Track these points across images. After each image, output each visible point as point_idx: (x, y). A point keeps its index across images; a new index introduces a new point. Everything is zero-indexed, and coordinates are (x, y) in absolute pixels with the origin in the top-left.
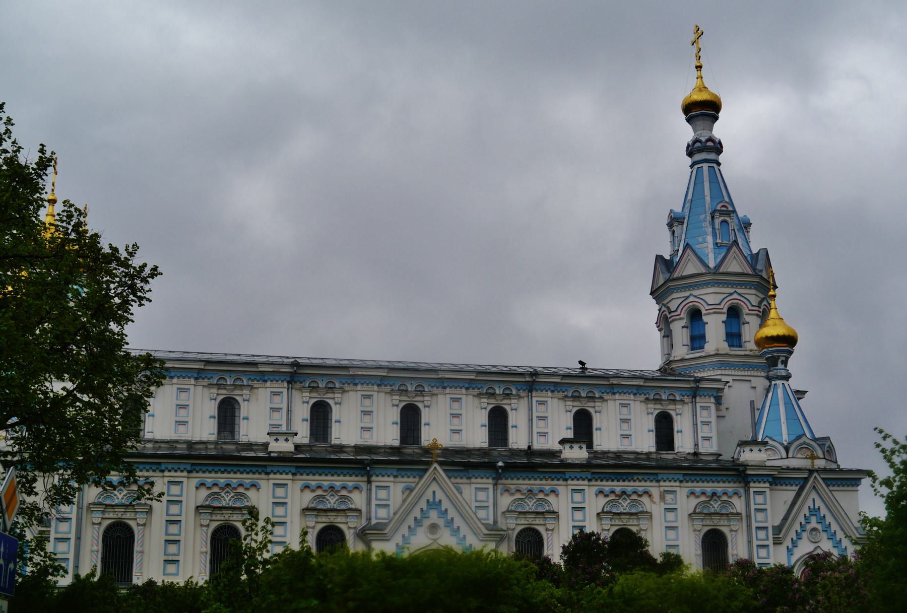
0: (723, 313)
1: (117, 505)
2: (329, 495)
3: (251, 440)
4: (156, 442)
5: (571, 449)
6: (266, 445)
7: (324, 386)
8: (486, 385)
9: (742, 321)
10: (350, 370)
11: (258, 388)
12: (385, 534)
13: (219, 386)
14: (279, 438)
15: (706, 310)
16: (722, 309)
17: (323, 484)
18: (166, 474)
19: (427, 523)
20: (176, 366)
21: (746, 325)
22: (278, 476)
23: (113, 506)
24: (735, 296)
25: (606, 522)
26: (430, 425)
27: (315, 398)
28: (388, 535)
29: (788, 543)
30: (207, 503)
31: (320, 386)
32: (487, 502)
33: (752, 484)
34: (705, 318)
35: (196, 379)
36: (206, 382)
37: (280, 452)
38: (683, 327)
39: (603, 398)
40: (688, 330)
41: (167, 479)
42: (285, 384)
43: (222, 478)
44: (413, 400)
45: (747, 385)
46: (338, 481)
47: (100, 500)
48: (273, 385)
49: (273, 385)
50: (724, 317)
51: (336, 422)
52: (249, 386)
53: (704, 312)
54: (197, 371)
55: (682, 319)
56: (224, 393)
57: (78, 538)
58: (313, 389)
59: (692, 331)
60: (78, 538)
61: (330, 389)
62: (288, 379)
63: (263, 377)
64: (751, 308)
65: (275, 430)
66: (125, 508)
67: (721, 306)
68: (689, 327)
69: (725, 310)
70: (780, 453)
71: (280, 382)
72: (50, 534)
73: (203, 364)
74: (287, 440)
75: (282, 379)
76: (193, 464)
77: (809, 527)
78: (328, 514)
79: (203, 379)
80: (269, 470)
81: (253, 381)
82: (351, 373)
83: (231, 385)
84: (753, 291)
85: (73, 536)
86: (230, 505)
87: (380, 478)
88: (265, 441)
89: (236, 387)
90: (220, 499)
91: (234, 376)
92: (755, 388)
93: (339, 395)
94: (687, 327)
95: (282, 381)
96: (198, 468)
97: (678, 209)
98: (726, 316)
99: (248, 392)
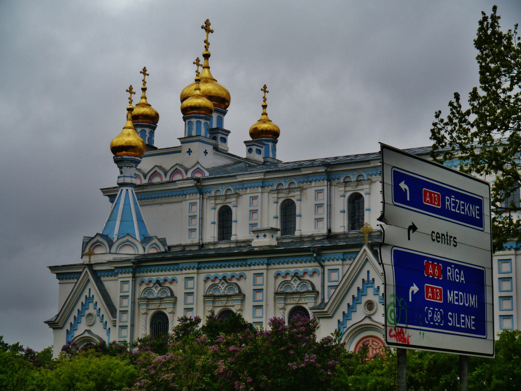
1: (155, 299)
2: (154, 287)
3: (303, 234)
4: (237, 242)
5: (265, 237)
6: (249, 242)
7: (355, 179)
8: (343, 174)
10: (371, 162)
11: (306, 189)
12: (326, 312)
13: (278, 191)
14: (259, 235)
17: (281, 271)
18: (184, 271)
19: (364, 299)
20: (245, 179)
22: (257, 267)
23: (152, 299)
25: (143, 308)
26: (371, 210)
27: (350, 190)
28: (329, 313)
29: (68, 327)
30: (211, 293)
31: (352, 180)
32: (262, 285)
33: (327, 263)
35: (263, 187)
36: (270, 188)
37: (260, 247)
39: (372, 180)
41: (184, 276)
42: (325, 182)
43: (220, 272)
44: (356, 189)
46: (300, 267)
47: (145, 295)
48: (317, 185)
49: (317, 185)
51: (366, 210)
52: (300, 187)
54: (261, 181)
56: (283, 196)
57: (133, 325)
58: (346, 183)
60: (133, 325)
61: (359, 182)
62: (261, 184)
63: (308, 178)
65: (255, 228)
66: (160, 300)
70: (135, 246)
71: (321, 181)
72: (116, 323)
73: (263, 174)
74: (265, 236)
75: (322, 178)
76: (199, 263)
77: (87, 312)
78: (293, 297)
79: (268, 186)
80: (249, 262)
81: (302, 183)
82: (372, 165)
83: (286, 189)
85: (129, 324)
86: (225, 293)
87: (331, 262)
88: (248, 238)
89: (290, 190)
90: (306, 285)
91: (288, 181)
93: (367, 186)
95: (323, 180)
96: (203, 265)
99: (298, 193)
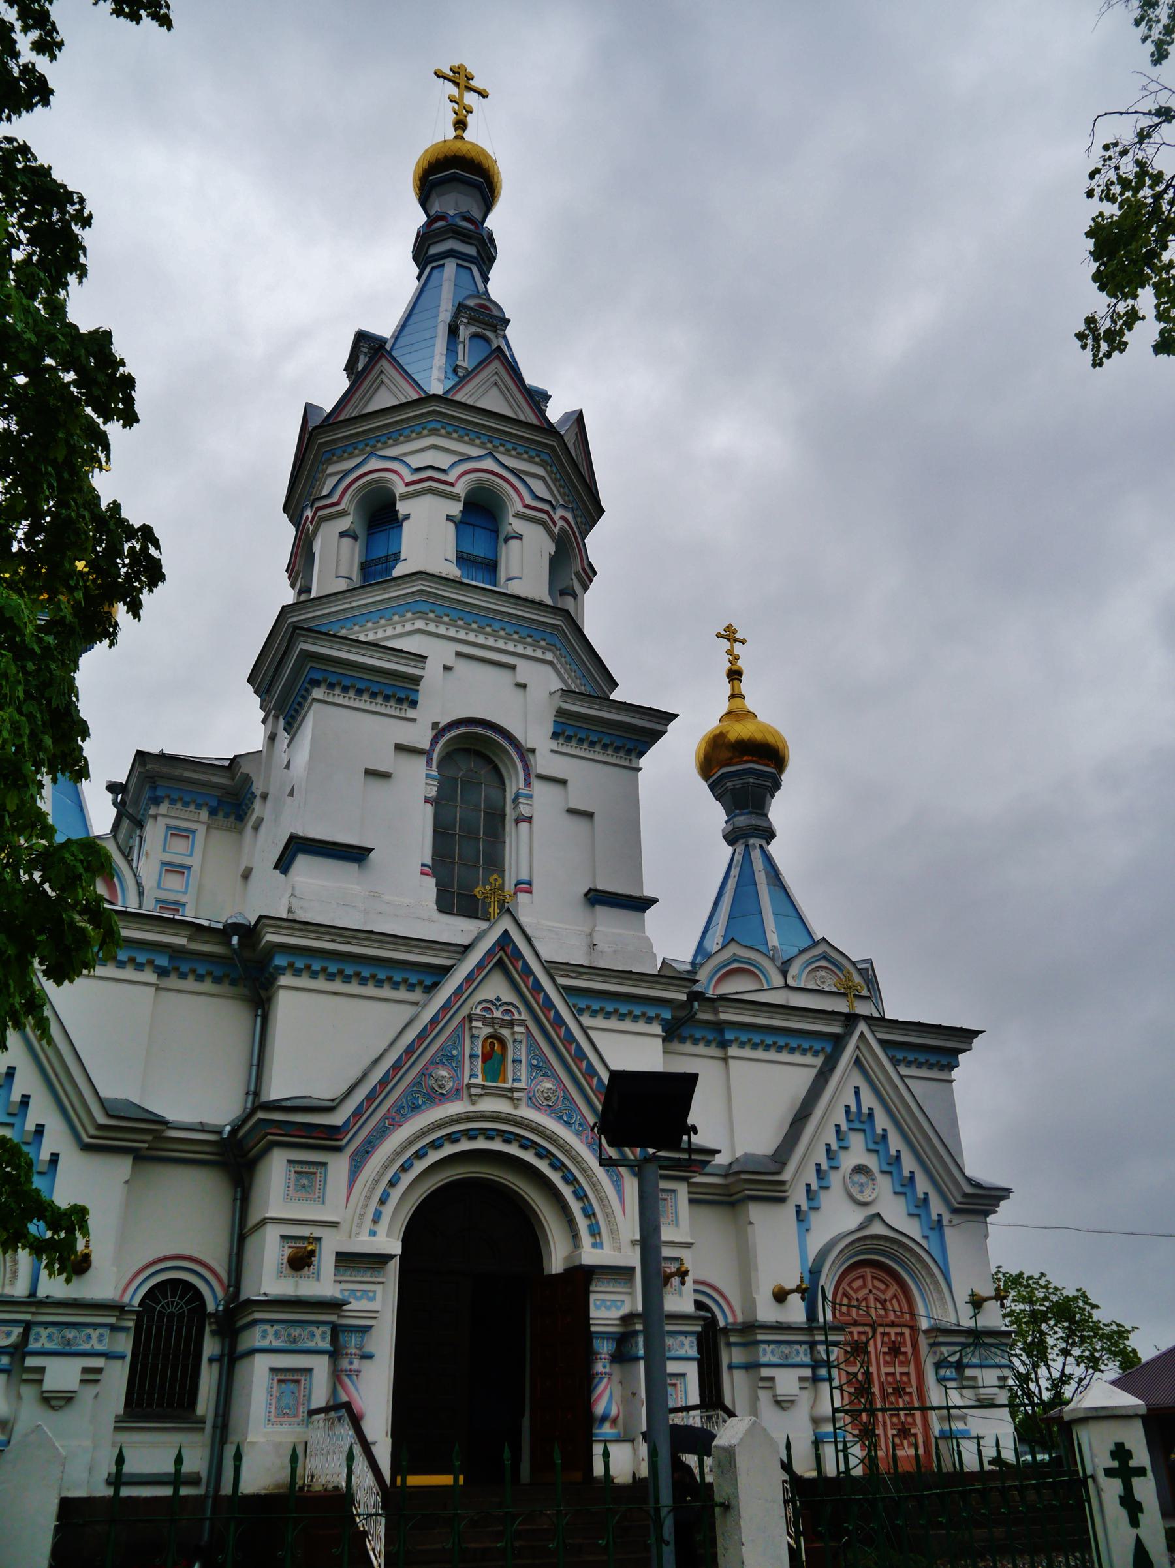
0: (454, 497)
9: (506, 530)
15: (408, 484)
16: (452, 484)
21: (514, 543)
24: (489, 464)
34: (402, 508)
38: (342, 535)
40: (358, 546)
45: (504, 676)
50: (456, 509)
53: (400, 489)
55: (343, 514)
59: (368, 548)
64: (529, 500)
67: (451, 478)
68: (361, 532)
69: (461, 489)
84: (540, 471)
92: (523, 686)
94: (355, 538)
97: (384, 328)
98: (460, 506)
